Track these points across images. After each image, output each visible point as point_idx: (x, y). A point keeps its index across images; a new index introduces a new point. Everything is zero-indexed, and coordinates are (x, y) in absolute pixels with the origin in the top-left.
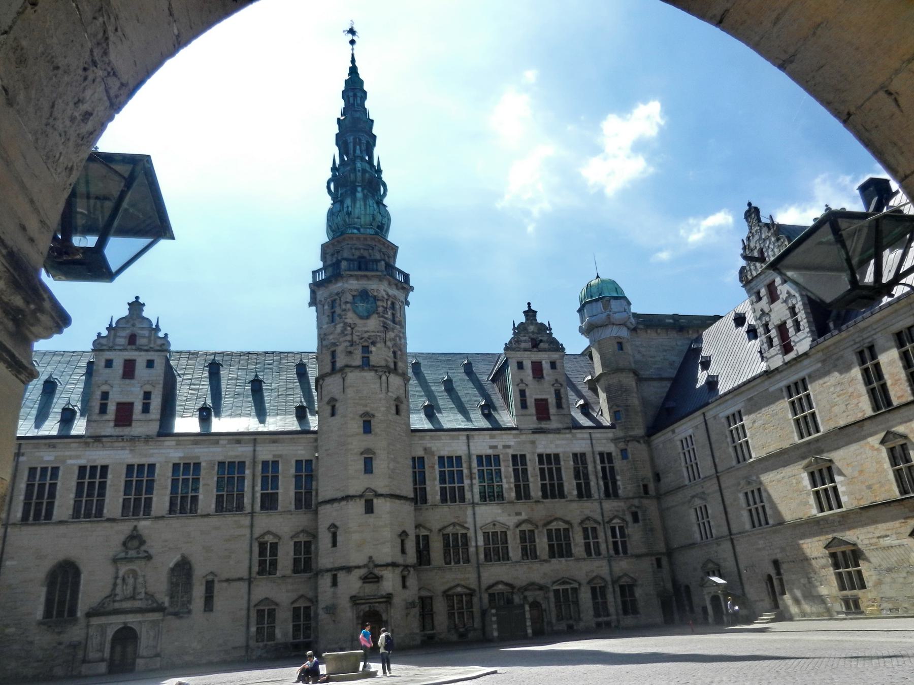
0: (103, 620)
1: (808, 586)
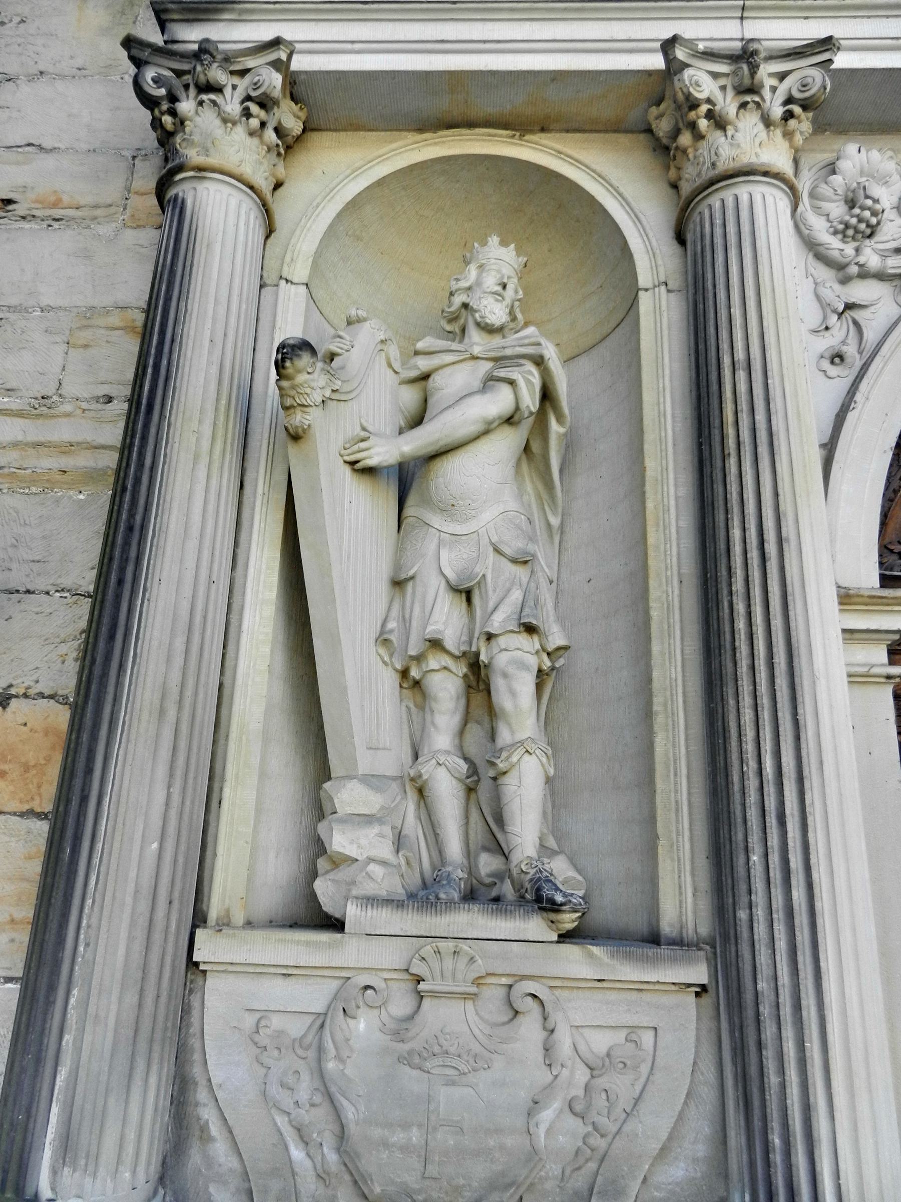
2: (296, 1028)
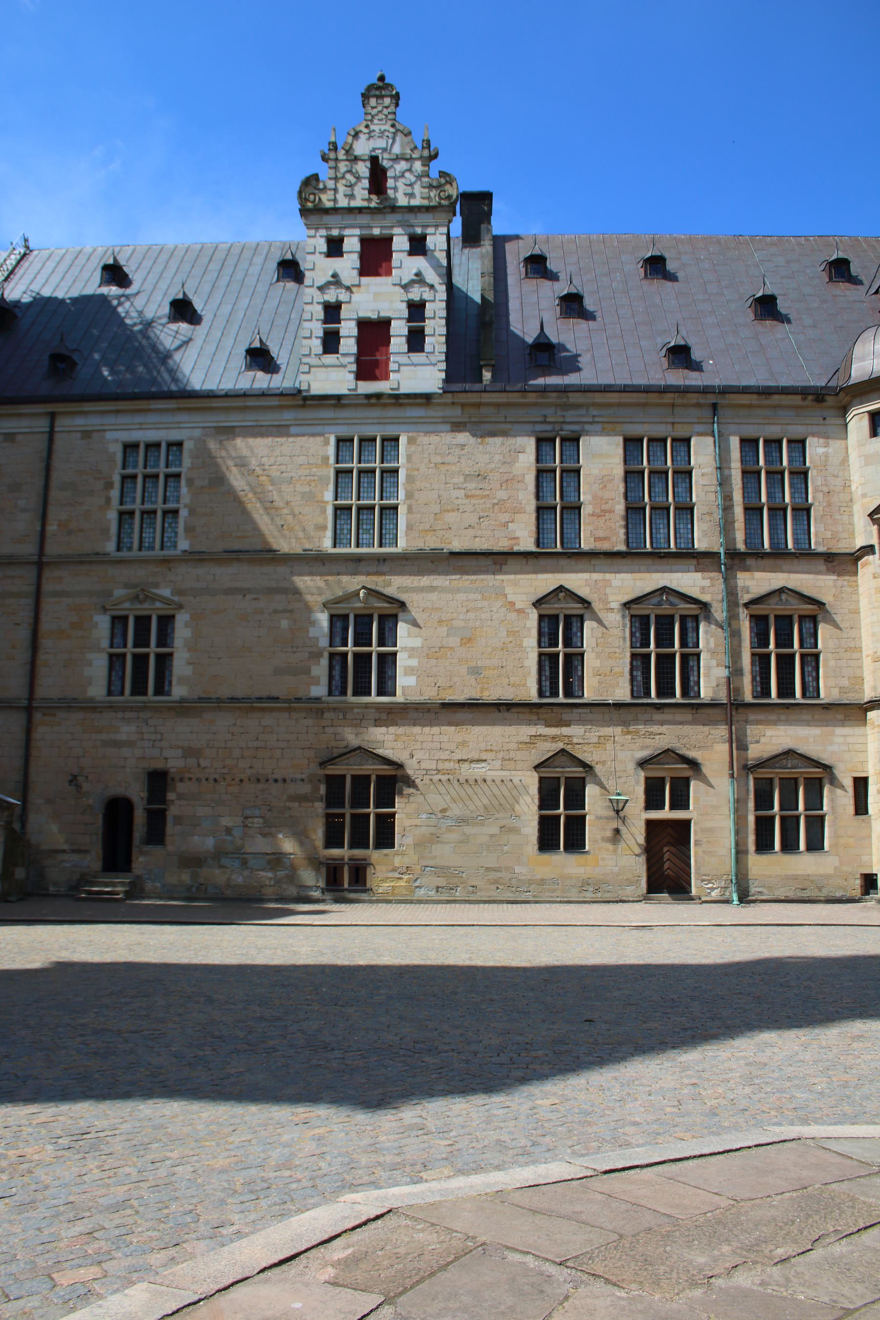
1: (237, 833)
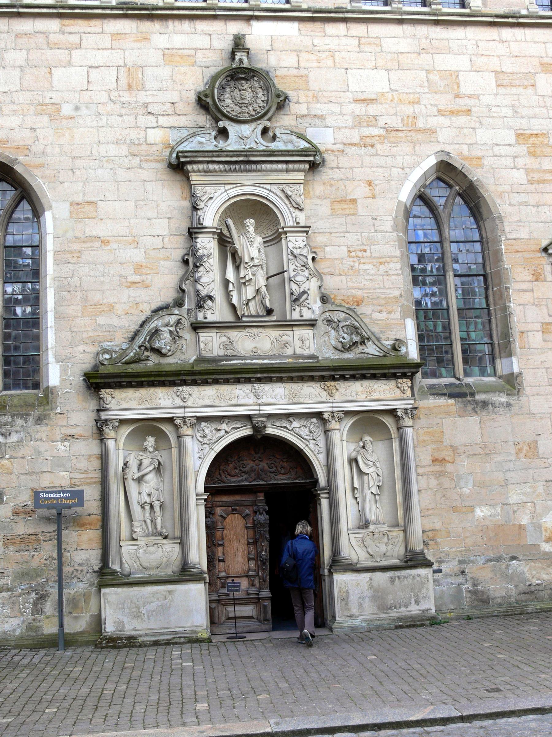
0: (161, 402)
2: (133, 551)
